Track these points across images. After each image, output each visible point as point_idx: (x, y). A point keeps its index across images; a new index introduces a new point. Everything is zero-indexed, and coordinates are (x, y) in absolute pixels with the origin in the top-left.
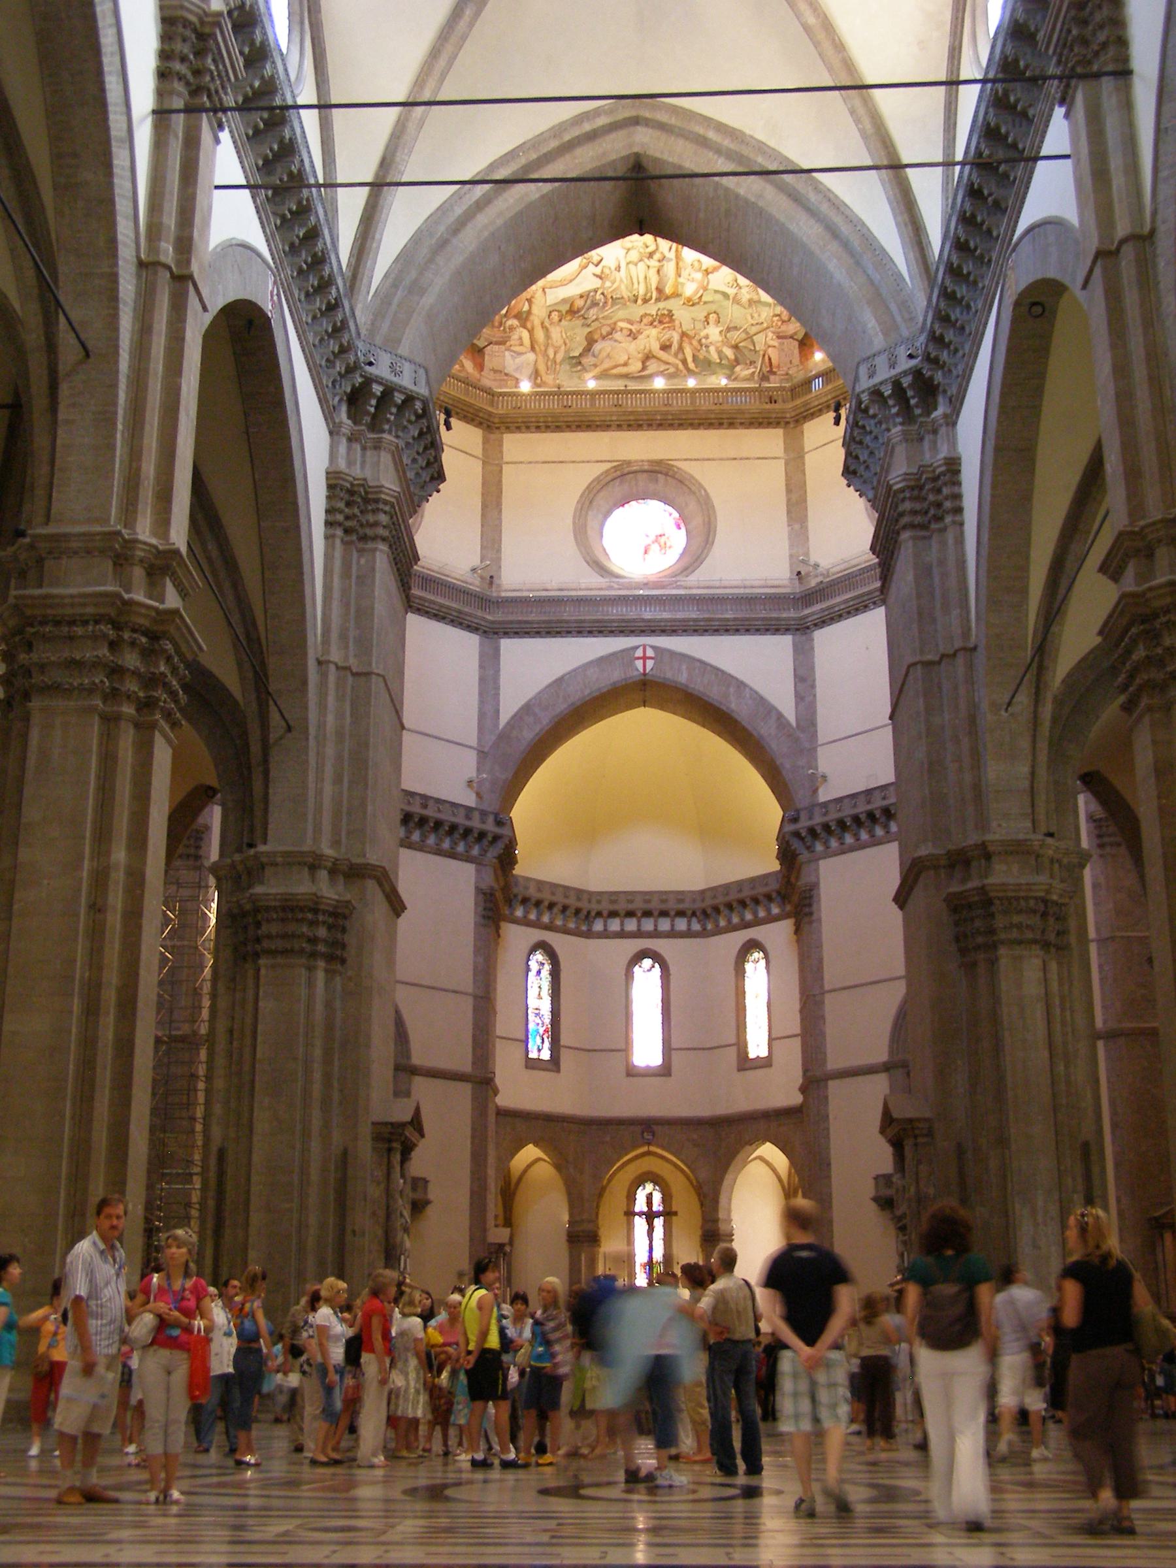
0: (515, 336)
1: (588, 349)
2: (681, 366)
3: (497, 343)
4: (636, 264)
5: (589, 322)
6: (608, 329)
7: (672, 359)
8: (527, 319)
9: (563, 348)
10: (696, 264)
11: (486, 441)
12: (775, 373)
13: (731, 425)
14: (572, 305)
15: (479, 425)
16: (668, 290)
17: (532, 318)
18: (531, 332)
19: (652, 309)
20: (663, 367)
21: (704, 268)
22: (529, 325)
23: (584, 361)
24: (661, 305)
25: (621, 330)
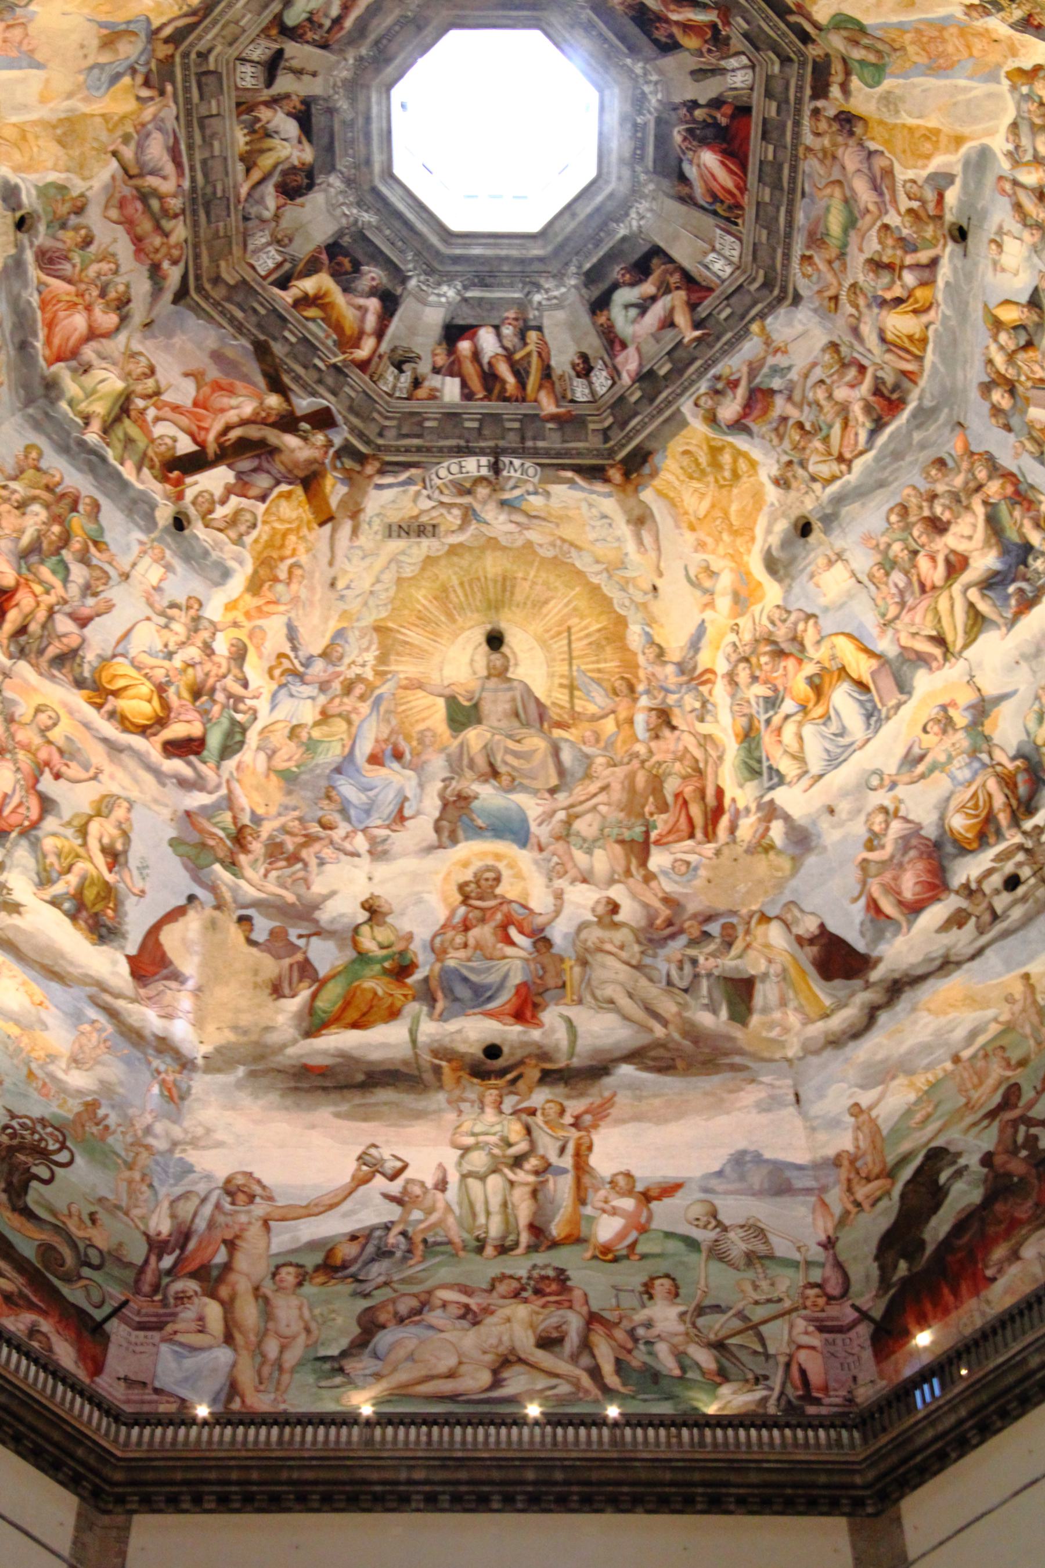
0: (188, 1314)
1: (362, 1343)
2: (586, 1381)
3: (142, 1327)
4: (482, 1178)
5: (368, 1287)
6: (414, 1303)
7: (564, 1367)
8: (220, 1279)
9: (302, 1339)
10: (621, 1181)
11: (83, 1525)
12: (817, 1402)
13: (716, 1505)
14: (330, 1253)
15: (72, 1482)
16: (556, 1229)
17: (232, 1277)
18: (228, 1306)
19: (520, 1266)
20: (542, 1382)
21: (640, 1187)
22: (224, 1292)
23: (349, 1365)
24: (540, 1258)
25: (444, 1305)
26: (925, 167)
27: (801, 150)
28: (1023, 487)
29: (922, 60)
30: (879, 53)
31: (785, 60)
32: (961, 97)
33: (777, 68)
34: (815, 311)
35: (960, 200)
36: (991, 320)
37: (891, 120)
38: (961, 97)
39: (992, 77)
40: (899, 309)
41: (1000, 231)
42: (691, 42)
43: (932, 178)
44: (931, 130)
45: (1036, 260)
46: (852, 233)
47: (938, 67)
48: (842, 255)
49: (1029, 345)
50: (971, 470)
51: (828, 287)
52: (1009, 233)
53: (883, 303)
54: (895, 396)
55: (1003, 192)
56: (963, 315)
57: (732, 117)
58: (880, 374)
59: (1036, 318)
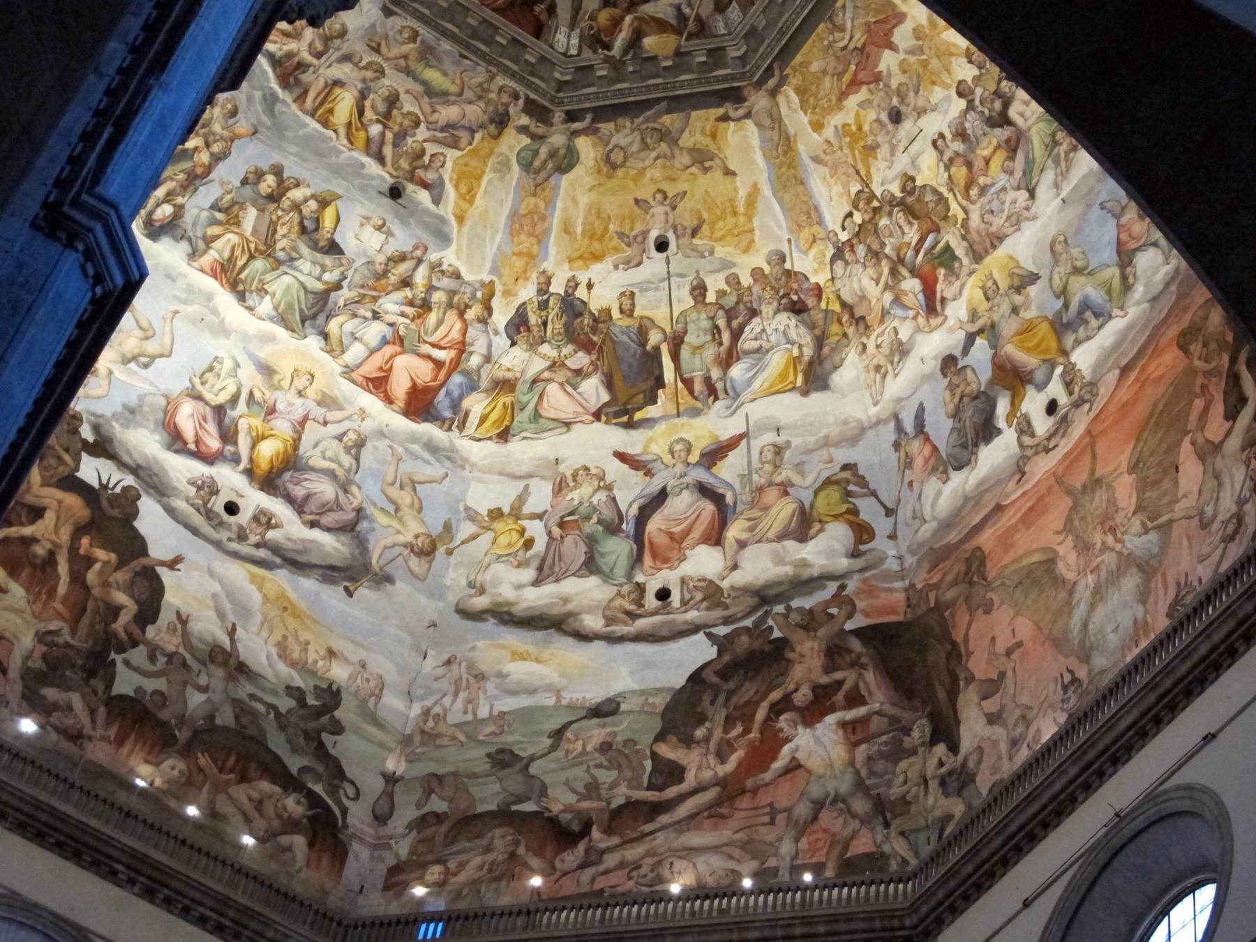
26: (451, 179)
27: (494, 69)
28: (198, 182)
29: (522, 211)
30: (537, 172)
31: (561, 86)
32: (489, 233)
33: (557, 75)
34: (373, 25)
35: (419, 204)
36: (328, 198)
37: (492, 162)
38: (489, 233)
39: (495, 270)
40: (355, 110)
41: (390, 234)
42: (604, 17)
43: (441, 182)
44: (474, 196)
45: (364, 260)
46: (419, 88)
47: (514, 217)
48: (408, 72)
49: (303, 230)
50: (222, 138)
51: (388, 46)
52: (386, 242)
53: (363, 96)
54: (291, 80)
55: (416, 248)
56: (338, 171)
57: (537, 19)
58: (311, 69)
59: (322, 244)
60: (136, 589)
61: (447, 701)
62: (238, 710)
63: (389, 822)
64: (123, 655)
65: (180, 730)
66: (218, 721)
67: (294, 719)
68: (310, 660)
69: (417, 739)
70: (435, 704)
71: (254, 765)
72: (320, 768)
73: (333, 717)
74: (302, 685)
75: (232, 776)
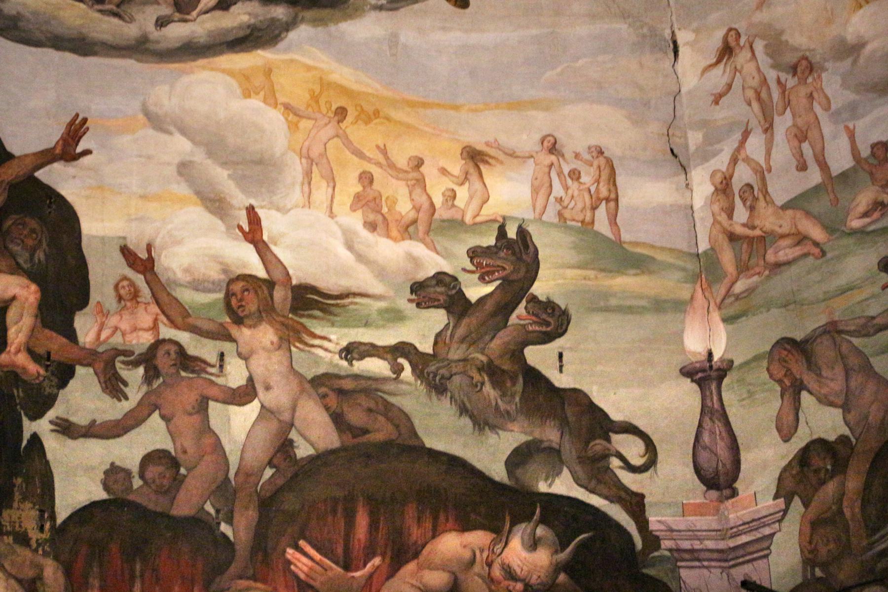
60: (16, 248)
61: (755, 146)
62: (332, 400)
63: (738, 485)
64: (51, 414)
65: (230, 521)
66: (303, 450)
67: (456, 353)
68: (438, 200)
69: (727, 259)
70: (734, 161)
71: (411, 512)
72: (551, 434)
73: (534, 299)
74: (446, 267)
75: (377, 561)
